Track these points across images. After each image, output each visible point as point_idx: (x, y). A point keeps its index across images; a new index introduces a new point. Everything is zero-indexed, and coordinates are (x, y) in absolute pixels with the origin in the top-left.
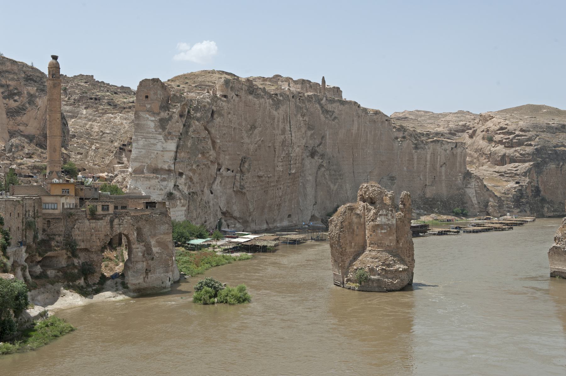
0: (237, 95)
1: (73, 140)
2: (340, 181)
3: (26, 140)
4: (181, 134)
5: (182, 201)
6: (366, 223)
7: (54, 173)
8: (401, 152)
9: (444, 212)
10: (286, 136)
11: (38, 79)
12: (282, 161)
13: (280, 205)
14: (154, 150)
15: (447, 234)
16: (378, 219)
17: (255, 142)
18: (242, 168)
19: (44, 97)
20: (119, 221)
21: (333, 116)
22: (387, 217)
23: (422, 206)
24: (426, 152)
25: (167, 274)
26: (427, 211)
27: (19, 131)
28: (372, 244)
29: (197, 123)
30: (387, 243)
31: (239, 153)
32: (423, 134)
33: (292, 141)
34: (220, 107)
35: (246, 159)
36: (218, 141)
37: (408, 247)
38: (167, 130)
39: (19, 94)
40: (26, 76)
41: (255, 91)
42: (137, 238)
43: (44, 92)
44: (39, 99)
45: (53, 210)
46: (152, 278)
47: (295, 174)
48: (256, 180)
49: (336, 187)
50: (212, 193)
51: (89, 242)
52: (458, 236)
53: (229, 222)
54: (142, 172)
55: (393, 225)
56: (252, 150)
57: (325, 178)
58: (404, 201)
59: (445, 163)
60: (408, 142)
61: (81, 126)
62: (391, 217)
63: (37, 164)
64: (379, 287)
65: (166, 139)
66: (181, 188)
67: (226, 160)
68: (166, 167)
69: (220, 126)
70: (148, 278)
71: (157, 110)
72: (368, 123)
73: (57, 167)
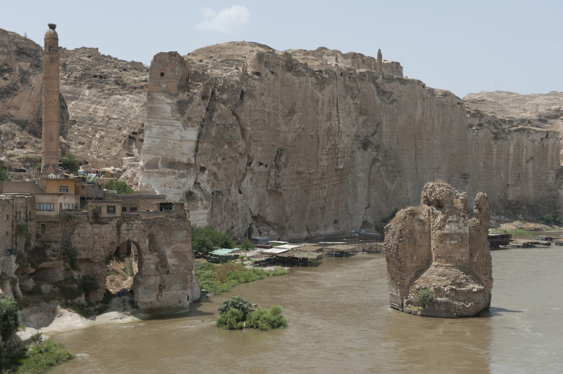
0: (272, 72)
1: (73, 126)
2: (399, 178)
3: (17, 127)
4: (203, 120)
5: (204, 202)
6: (431, 232)
7: (51, 167)
8: (476, 143)
9: (531, 219)
10: (332, 122)
11: (33, 52)
13: (324, 208)
14: (170, 139)
15: (534, 247)
16: (447, 226)
17: (295, 131)
18: (277, 162)
19: (39, 75)
20: (128, 226)
21: (391, 99)
22: (458, 224)
23: (503, 211)
24: (509, 143)
25: (185, 291)
26: (509, 218)
27: (9, 116)
28: (439, 257)
29: (223, 106)
30: (458, 257)
31: (274, 144)
32: (504, 121)
33: (339, 129)
34: (251, 87)
35: (283, 151)
36: (249, 129)
37: (484, 262)
38: (186, 115)
39: (10, 70)
40: (18, 49)
41: (294, 67)
42: (149, 247)
43: (39, 69)
44: (33, 77)
45: (48, 212)
46: (167, 296)
47: (342, 169)
48: (294, 176)
49: (394, 186)
50: (240, 193)
51: (92, 250)
52: (548, 249)
53: (261, 228)
54: (156, 167)
55: (465, 234)
56: (290, 140)
57: (381, 175)
58: (480, 204)
59: (532, 158)
60: (486, 130)
61: (83, 110)
62: (463, 224)
63: (31, 156)
64: (447, 311)
65: (185, 126)
66: (203, 186)
67: (258, 153)
68: (185, 160)
69: (250, 111)
70: (161, 296)
71: (174, 91)
72: (435, 107)
73: (54, 159)
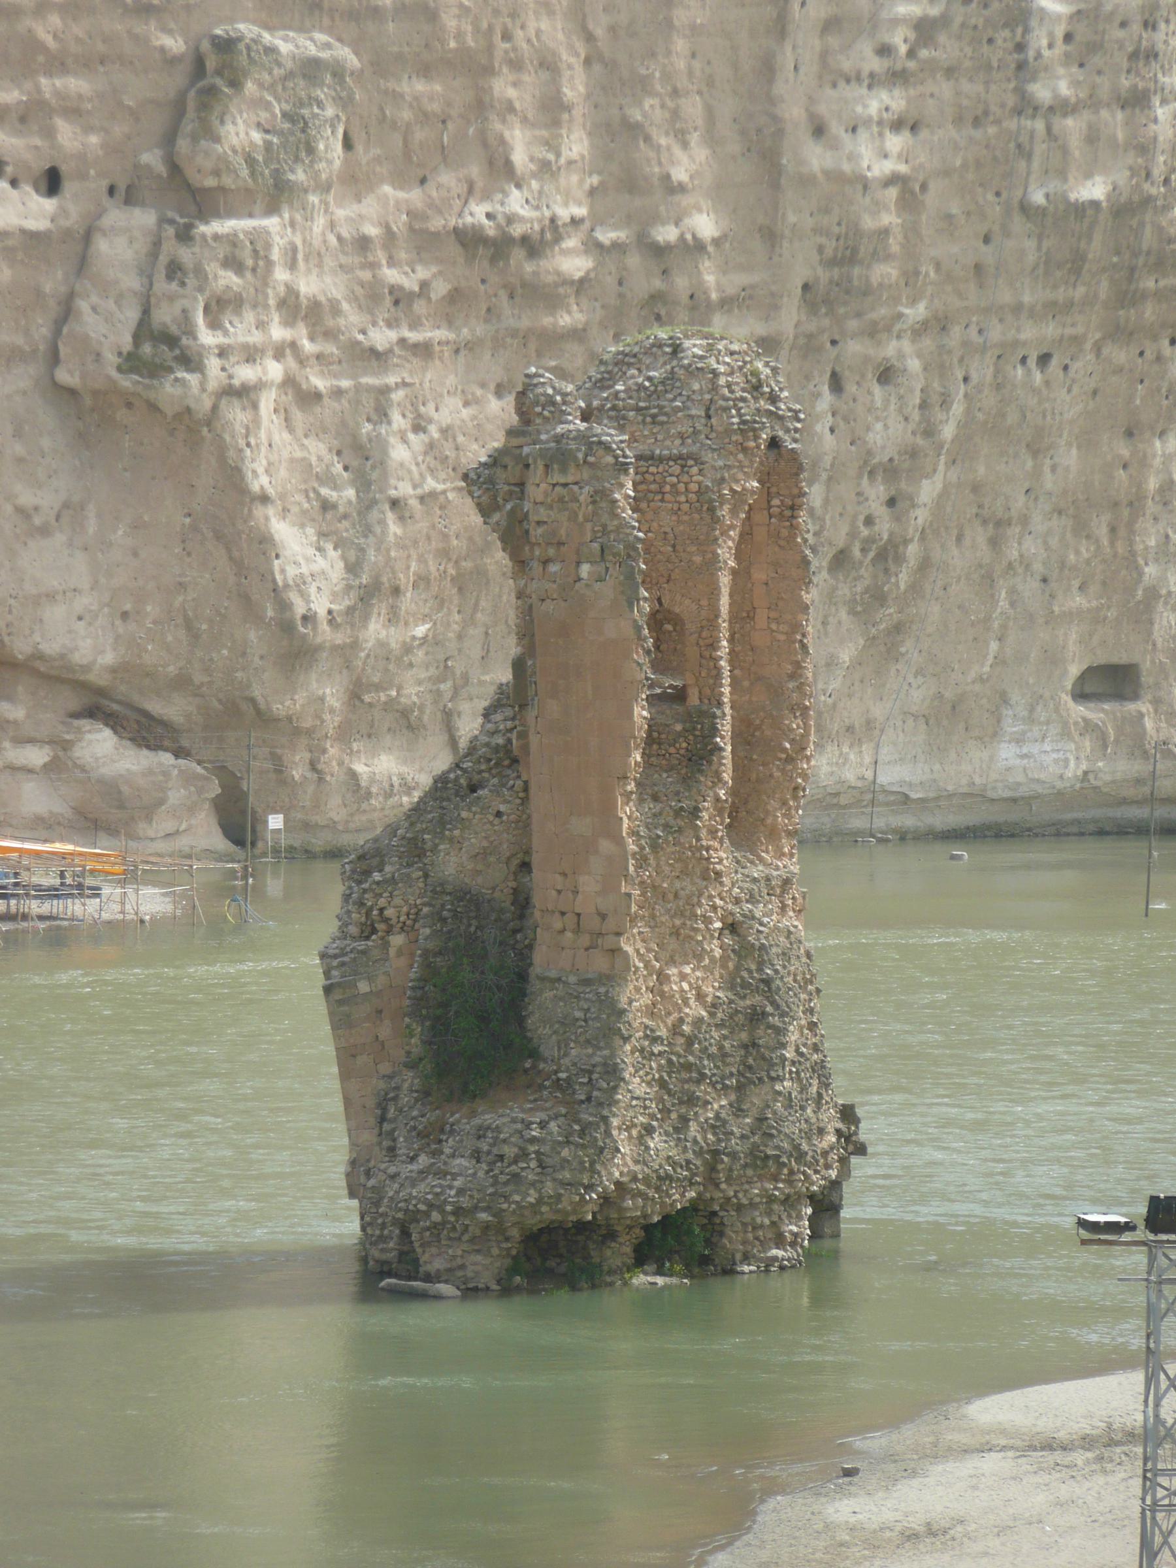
12: (898, 77)
18: (183, 145)
